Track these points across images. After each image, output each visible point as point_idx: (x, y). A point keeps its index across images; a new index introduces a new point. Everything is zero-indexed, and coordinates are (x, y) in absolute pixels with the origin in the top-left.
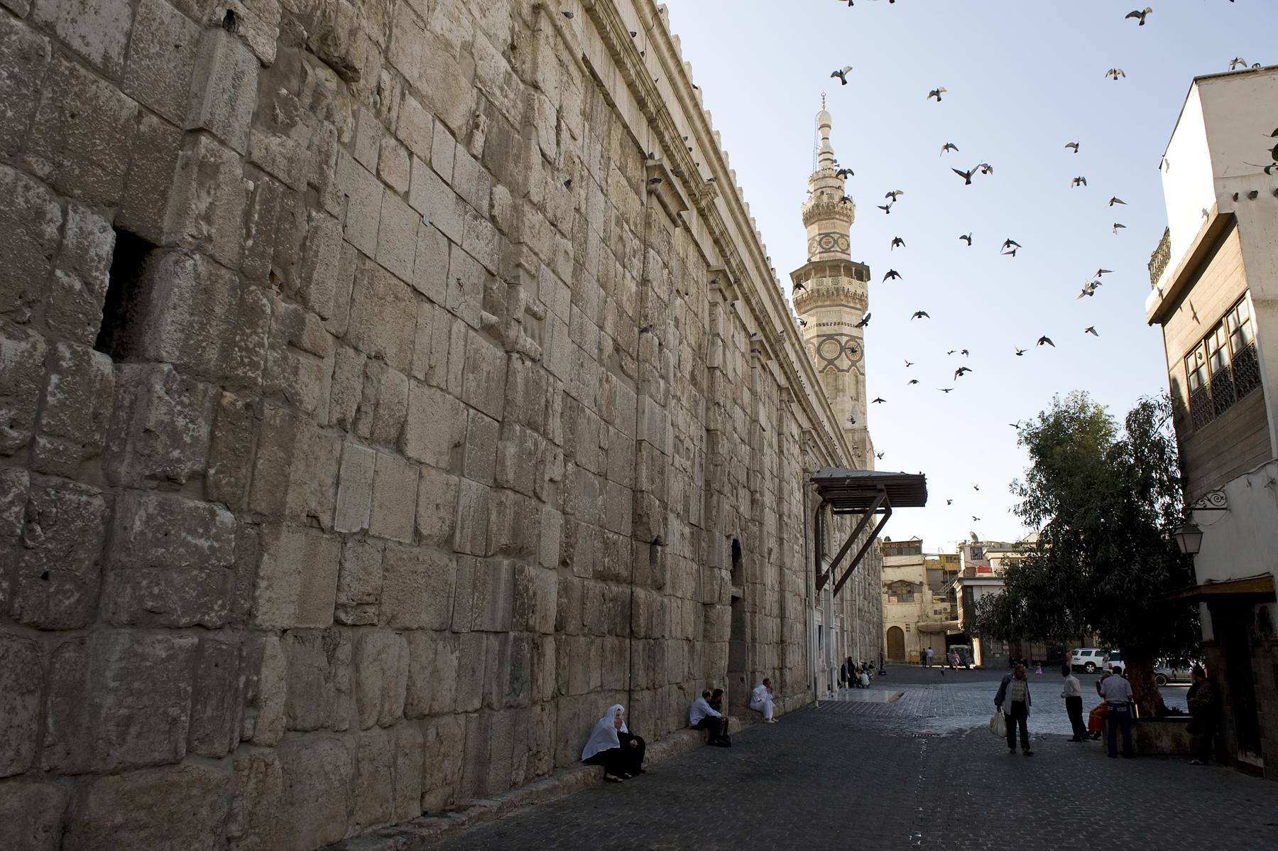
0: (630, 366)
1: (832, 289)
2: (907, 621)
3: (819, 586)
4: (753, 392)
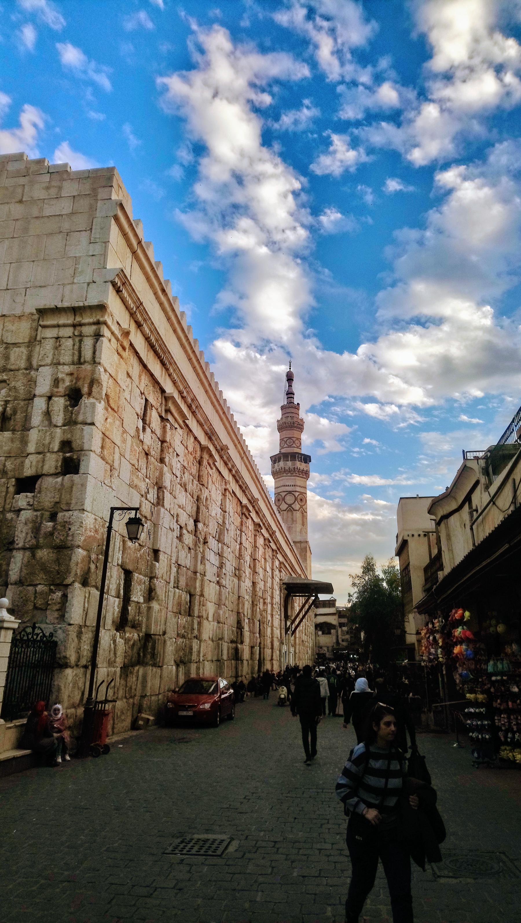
0: (237, 572)
1: (292, 467)
2: (328, 645)
4: (265, 559)
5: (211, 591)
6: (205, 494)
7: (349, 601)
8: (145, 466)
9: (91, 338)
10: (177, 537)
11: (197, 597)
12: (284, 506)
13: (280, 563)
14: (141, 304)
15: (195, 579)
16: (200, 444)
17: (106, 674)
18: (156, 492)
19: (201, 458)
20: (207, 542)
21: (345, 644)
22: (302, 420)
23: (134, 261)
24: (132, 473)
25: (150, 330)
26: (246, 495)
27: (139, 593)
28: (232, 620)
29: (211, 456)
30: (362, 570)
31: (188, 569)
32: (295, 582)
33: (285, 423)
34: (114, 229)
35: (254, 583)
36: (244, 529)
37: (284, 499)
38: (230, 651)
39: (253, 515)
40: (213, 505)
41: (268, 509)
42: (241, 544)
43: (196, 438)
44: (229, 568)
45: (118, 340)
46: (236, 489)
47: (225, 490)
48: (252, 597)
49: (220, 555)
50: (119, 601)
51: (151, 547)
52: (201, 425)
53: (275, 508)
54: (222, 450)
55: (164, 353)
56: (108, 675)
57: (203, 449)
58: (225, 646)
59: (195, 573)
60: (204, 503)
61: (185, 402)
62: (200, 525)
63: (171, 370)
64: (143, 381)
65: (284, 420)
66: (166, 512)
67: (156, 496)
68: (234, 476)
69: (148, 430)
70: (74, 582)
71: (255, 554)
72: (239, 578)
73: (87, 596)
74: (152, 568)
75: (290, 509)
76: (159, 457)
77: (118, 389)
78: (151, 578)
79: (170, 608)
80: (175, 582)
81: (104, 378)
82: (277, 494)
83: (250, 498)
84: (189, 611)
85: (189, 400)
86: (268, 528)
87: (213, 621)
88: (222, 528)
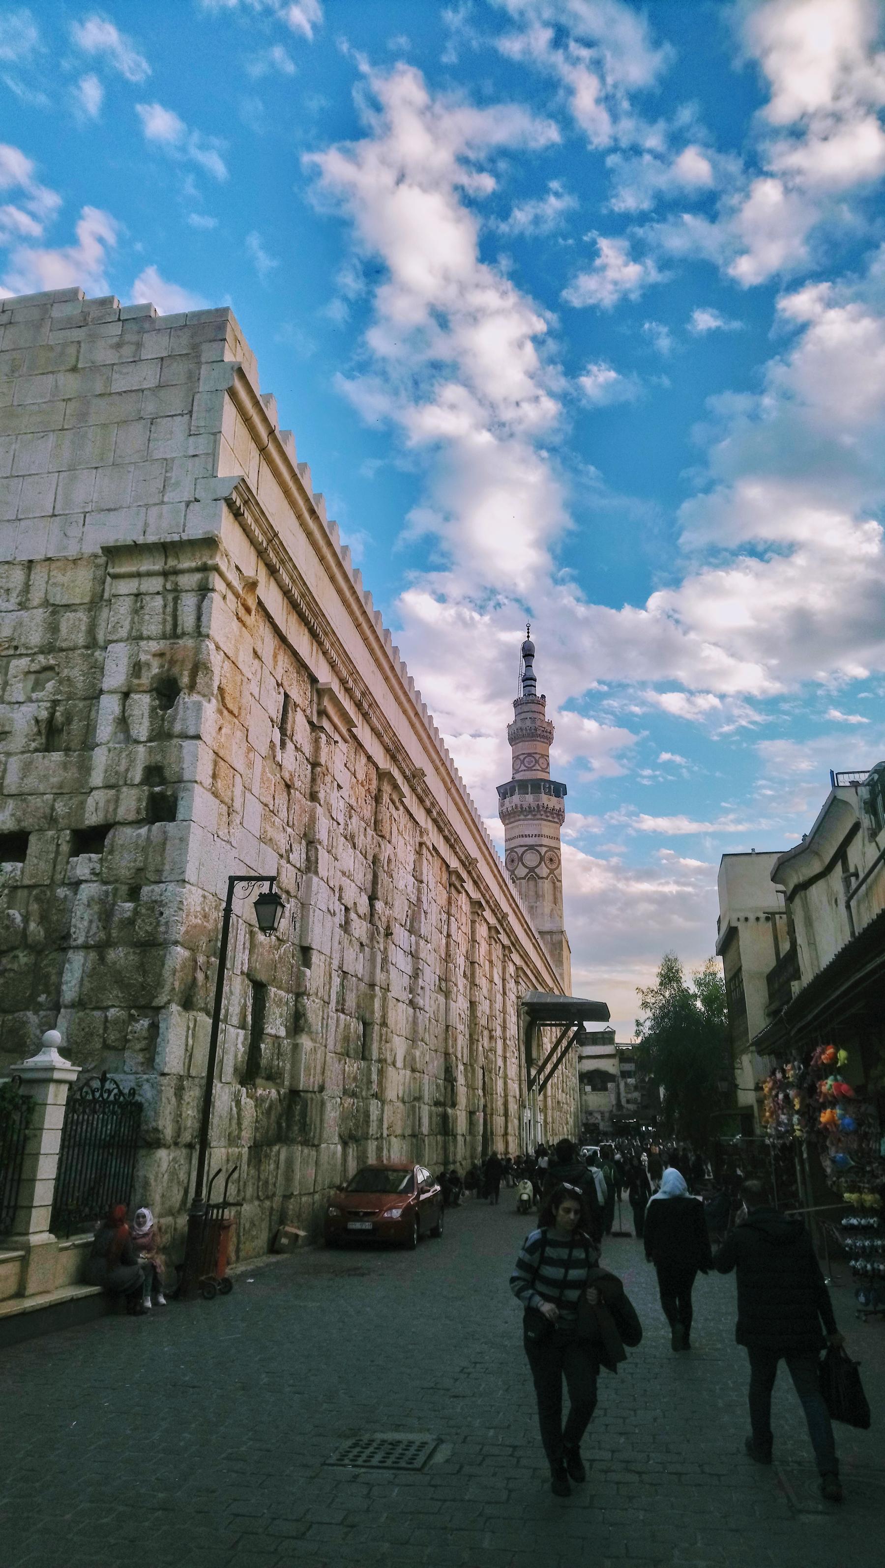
0: (443, 984)
2: (602, 1109)
3: (529, 1089)
4: (491, 962)
5: (400, 1017)
6: (387, 851)
7: (638, 1034)
8: (285, 806)
9: (193, 594)
10: (341, 925)
11: (376, 1028)
12: (521, 871)
13: (518, 968)
14: (276, 535)
15: (373, 997)
16: (377, 768)
17: (224, 1157)
18: (304, 850)
19: (379, 790)
20: (391, 934)
21: (631, 1107)
22: (550, 724)
23: (264, 464)
24: (264, 818)
25: (291, 578)
26: (456, 853)
27: (279, 1021)
28: (435, 1066)
29: (396, 787)
30: (658, 980)
31: (359, 979)
32: (543, 1000)
34: (229, 410)
35: (473, 1004)
36: (453, 910)
37: (521, 859)
38: (434, 1119)
39: (469, 886)
40: (401, 871)
41: (495, 876)
42: (449, 936)
43: (369, 758)
44: (429, 977)
45: (237, 596)
46: (439, 842)
47: (421, 844)
48: (470, 1027)
49: (414, 955)
50: (246, 1035)
51: (297, 942)
52: (379, 736)
53: (506, 875)
54: (414, 777)
55: (315, 616)
56: (228, 1160)
57: (383, 775)
58: (425, 1111)
59: (372, 985)
60: (386, 868)
61: (352, 697)
62: (379, 905)
63: (327, 645)
64: (280, 663)
65: (519, 724)
66: (322, 883)
67: (304, 856)
68: (435, 821)
69: (290, 746)
70: (169, 1002)
71: (473, 953)
72: (447, 994)
73: (191, 1026)
74: (299, 978)
75: (533, 876)
76: (308, 791)
77: (238, 678)
78: (299, 995)
79: (331, 1046)
80: (338, 1002)
81: (216, 660)
82: (510, 851)
83: (463, 858)
84: (363, 1052)
85: (358, 695)
86: (495, 909)
87: (405, 1067)
88: (416, 908)
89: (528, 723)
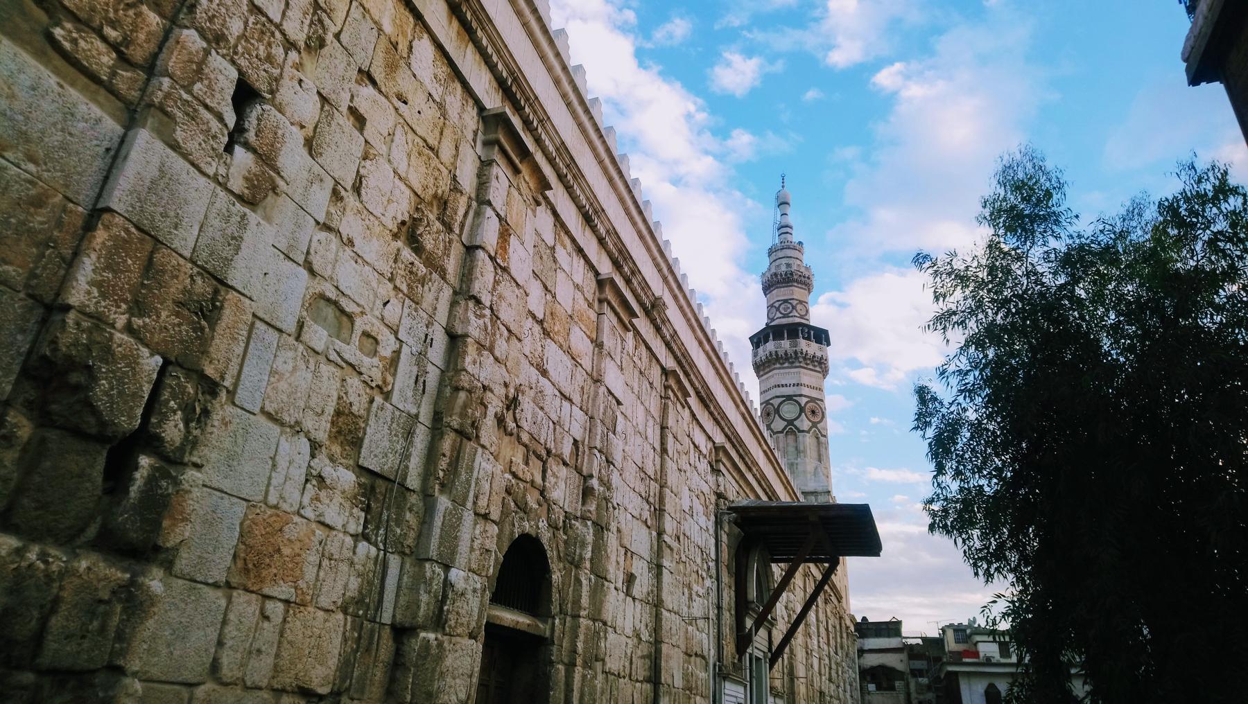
1: (790, 351)
12: (779, 425)
22: (807, 268)
33: (776, 274)
37: (777, 411)
53: (763, 427)
65: (773, 270)
75: (791, 429)
82: (766, 403)
89: (784, 268)
